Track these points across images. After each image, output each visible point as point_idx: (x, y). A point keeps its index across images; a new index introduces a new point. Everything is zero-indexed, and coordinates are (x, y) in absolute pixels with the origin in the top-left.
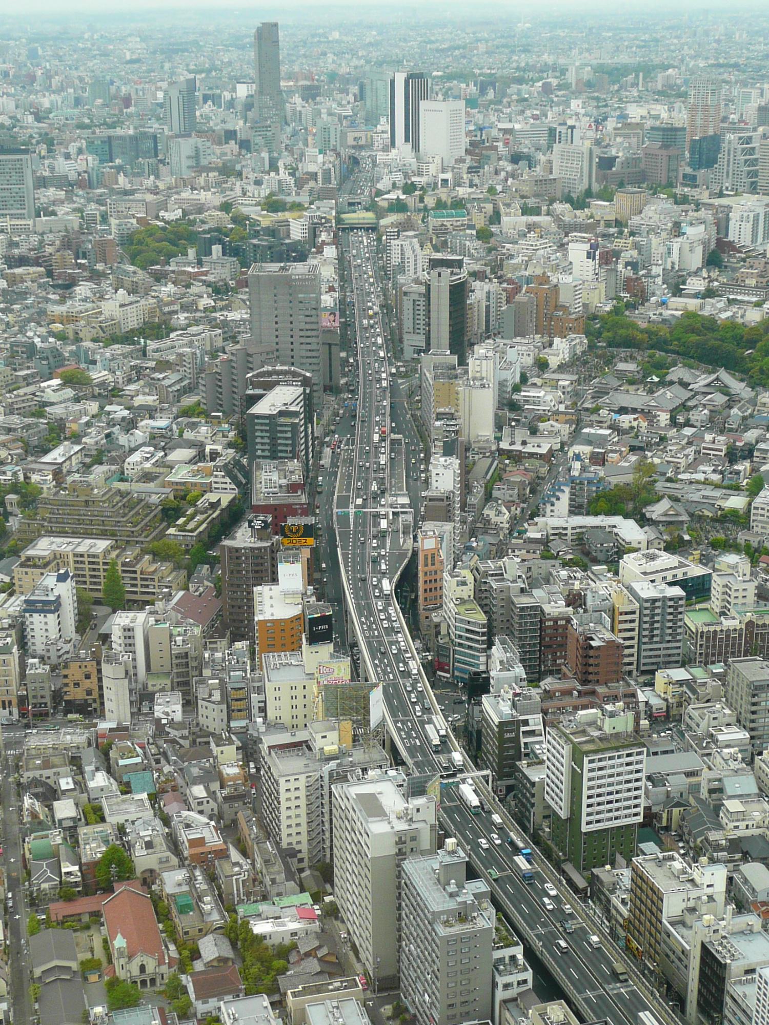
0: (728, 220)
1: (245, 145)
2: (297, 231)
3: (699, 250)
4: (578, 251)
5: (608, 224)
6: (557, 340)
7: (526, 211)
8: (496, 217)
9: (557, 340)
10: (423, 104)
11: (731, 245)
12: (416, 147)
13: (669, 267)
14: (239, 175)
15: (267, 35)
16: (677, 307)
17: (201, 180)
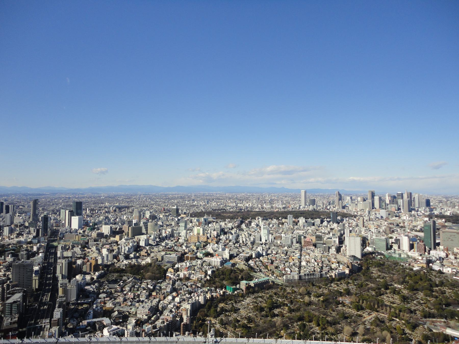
0: (140, 240)
1: (27, 227)
2: (35, 249)
3: (133, 248)
4: (105, 252)
5: (114, 243)
6: (96, 273)
7: (95, 241)
8: (87, 243)
9: (96, 273)
10: (72, 217)
11: (141, 247)
12: (71, 226)
13: (126, 252)
14: (23, 235)
15: (36, 202)
16: (126, 262)
17: (12, 237)
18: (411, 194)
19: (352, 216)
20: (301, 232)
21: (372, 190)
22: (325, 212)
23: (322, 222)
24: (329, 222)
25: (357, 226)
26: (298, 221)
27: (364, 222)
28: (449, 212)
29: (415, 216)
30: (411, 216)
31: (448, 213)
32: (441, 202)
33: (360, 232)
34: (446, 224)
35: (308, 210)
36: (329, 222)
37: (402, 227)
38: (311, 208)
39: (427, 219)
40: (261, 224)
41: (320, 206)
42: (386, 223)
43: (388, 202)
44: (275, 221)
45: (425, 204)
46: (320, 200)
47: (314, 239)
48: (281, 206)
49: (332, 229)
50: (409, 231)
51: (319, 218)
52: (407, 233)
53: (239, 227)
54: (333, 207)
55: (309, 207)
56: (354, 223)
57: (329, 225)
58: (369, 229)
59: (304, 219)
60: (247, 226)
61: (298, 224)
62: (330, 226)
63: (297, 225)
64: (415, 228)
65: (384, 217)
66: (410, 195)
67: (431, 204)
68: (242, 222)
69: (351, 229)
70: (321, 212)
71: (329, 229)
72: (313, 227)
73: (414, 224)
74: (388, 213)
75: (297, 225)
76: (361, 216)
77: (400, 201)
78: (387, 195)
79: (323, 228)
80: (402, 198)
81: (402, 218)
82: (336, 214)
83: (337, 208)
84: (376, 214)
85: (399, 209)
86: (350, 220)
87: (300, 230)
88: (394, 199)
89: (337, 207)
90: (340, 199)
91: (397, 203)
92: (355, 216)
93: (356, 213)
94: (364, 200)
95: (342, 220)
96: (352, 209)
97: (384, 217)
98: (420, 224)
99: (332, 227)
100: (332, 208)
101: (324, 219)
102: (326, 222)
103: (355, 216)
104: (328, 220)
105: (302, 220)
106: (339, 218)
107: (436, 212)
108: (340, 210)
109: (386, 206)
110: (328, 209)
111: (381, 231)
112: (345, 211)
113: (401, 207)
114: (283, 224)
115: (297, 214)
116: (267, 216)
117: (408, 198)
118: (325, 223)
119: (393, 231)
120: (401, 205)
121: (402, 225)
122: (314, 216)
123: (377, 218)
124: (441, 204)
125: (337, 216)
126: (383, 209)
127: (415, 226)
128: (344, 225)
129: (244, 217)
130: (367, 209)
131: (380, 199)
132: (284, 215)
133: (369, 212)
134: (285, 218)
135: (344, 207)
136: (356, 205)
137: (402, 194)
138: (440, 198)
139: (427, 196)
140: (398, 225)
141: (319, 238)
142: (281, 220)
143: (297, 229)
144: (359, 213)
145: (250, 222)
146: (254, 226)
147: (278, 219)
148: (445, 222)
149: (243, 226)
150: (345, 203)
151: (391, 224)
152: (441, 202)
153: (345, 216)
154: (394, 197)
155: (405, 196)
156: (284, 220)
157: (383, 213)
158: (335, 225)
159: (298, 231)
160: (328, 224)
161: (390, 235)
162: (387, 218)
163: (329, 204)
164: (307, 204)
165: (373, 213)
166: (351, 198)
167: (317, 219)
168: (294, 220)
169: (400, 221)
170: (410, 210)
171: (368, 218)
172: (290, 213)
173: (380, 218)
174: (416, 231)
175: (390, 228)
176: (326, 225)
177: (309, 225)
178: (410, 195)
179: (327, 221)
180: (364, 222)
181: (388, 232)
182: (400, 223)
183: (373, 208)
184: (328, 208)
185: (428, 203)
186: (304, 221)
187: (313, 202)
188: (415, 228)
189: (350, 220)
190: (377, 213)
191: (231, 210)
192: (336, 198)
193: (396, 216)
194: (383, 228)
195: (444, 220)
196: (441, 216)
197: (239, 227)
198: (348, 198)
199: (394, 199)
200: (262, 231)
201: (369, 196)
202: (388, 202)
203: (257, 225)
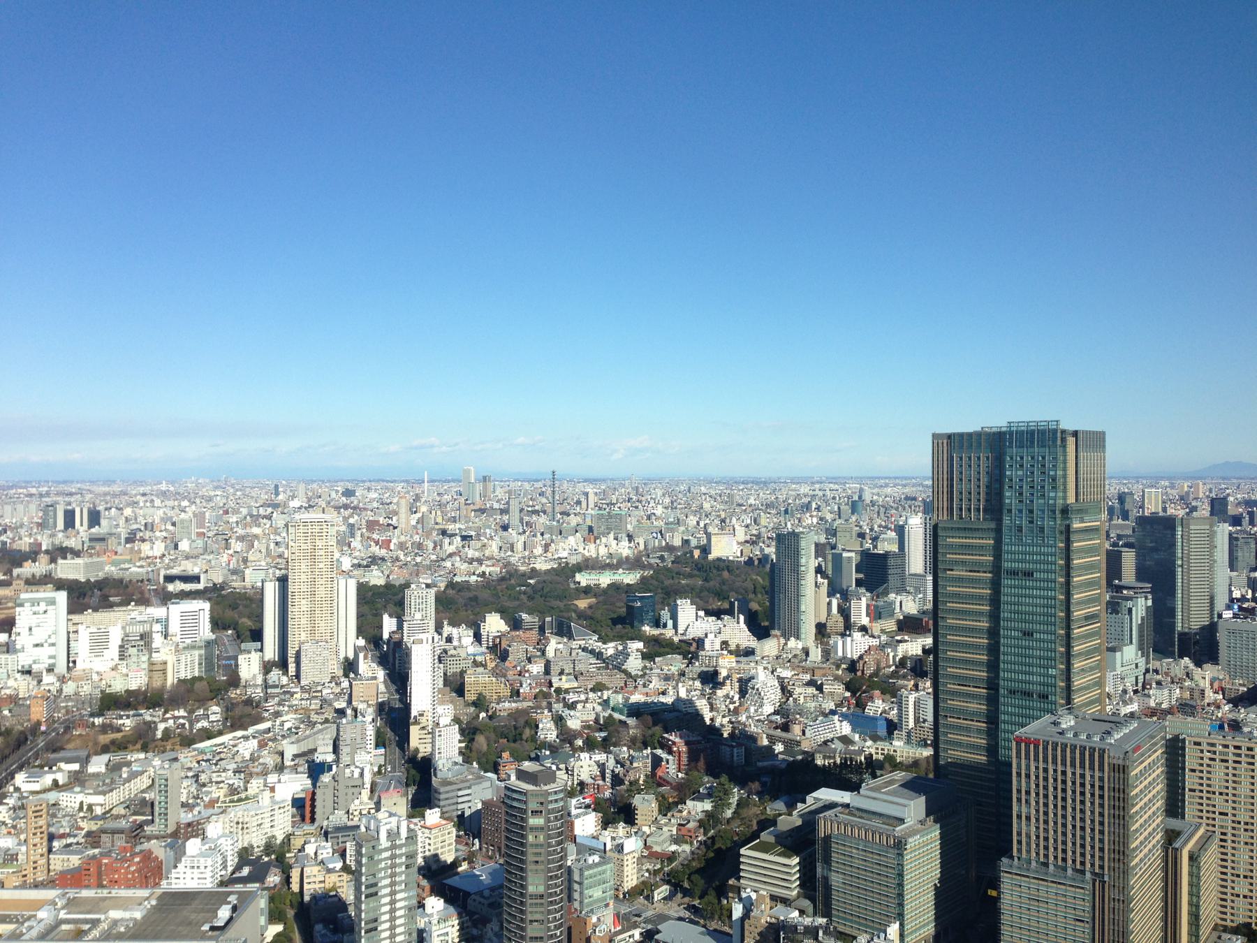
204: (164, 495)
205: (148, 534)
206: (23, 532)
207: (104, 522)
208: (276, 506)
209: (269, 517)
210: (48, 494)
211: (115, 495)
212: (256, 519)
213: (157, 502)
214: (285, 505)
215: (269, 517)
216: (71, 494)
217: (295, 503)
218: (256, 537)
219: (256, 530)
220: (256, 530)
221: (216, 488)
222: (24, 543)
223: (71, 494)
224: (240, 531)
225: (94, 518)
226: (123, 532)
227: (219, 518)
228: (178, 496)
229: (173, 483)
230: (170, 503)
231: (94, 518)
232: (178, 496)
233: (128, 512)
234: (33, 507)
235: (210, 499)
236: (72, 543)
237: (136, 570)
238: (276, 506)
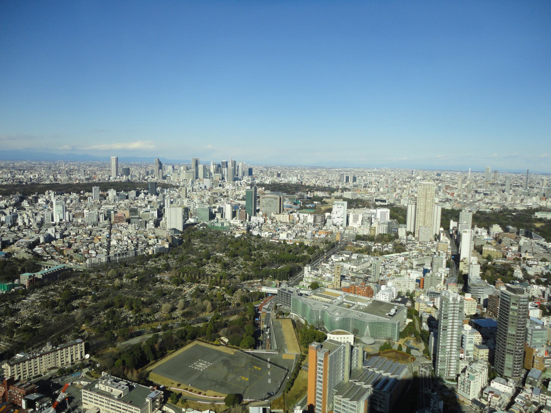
18: (235, 162)
19: (174, 187)
20: (111, 207)
21: (196, 158)
22: (142, 183)
23: (138, 194)
24: (146, 194)
25: (179, 197)
26: (108, 195)
27: (186, 193)
28: (269, 180)
29: (237, 185)
30: (234, 185)
31: (267, 182)
32: (262, 171)
33: (183, 203)
34: (265, 192)
35: (120, 182)
36: (146, 194)
37: (225, 196)
38: (124, 179)
39: (249, 188)
40: (54, 200)
41: (136, 175)
42: (209, 193)
43: (212, 171)
44: (74, 195)
45: (247, 173)
46: (137, 169)
47: (127, 214)
48: (83, 177)
49: (150, 202)
50: (232, 200)
51: (135, 190)
52: (230, 202)
53: (18, 205)
54: (152, 177)
55: (121, 178)
56: (176, 195)
57: (146, 198)
58: (192, 199)
59: (115, 191)
60: (30, 203)
61: (107, 198)
62: (148, 198)
63: (105, 199)
64: (238, 197)
65: (208, 187)
66: (234, 163)
67: (253, 173)
68: (22, 199)
69: (172, 200)
70: (138, 183)
71: (146, 202)
72: (127, 200)
73: (237, 193)
74: (211, 183)
75: (105, 199)
76: (183, 186)
77: (225, 170)
78: (212, 163)
79: (139, 202)
80: (227, 166)
81: (226, 188)
82: (156, 185)
83: (156, 179)
84: (199, 184)
85: (223, 178)
86: (171, 192)
87: (110, 205)
88: (219, 168)
89: (156, 178)
90: (161, 167)
91: (221, 172)
92: (177, 187)
93: (178, 184)
94: (187, 169)
95: (162, 191)
96: (173, 179)
97: (208, 187)
98: (242, 193)
99: (150, 200)
100: (151, 178)
101: (141, 190)
102: (143, 194)
103: (177, 187)
104: (145, 191)
105: (112, 193)
106: (158, 189)
107: (257, 181)
108: (160, 181)
109: (210, 175)
110: (145, 180)
111: (205, 201)
112: (166, 181)
113: (226, 178)
114: (86, 198)
115: (105, 187)
116: (61, 189)
117: (232, 166)
118: (142, 196)
119: (217, 201)
120: (226, 174)
121: (225, 194)
122: (129, 188)
123: (201, 188)
124: (262, 174)
125: (156, 187)
126: (207, 178)
127: (237, 195)
128: (164, 196)
129: (27, 191)
130: (191, 179)
131: (204, 168)
132: (88, 187)
133: (193, 182)
134: (89, 192)
135: (164, 178)
136: (179, 174)
137: (227, 162)
138: (261, 168)
139: (250, 166)
140: (221, 195)
141: (134, 211)
142: (83, 194)
143: (105, 204)
144: (182, 184)
145: (36, 199)
146: (42, 203)
147: (78, 192)
148: (265, 190)
149: (25, 203)
150: (165, 173)
151: (214, 193)
152: (262, 171)
153: (165, 186)
154: (219, 166)
155: (230, 164)
156: (87, 194)
157: (207, 182)
158: (154, 197)
159: (106, 206)
160: (145, 197)
161: (213, 205)
162: (211, 188)
163: (148, 174)
164: (119, 174)
165: (197, 183)
166: (173, 167)
167: (132, 191)
168: (101, 193)
169: (224, 190)
170: (235, 179)
171: (191, 188)
172: (96, 184)
173: (203, 188)
174: (239, 200)
175: (214, 198)
176: (143, 197)
177: (121, 199)
178: (234, 163)
179: (145, 193)
180: (186, 193)
181: (211, 202)
182: (224, 193)
183: (197, 178)
184: (146, 178)
185: (250, 172)
186: (115, 194)
187: (127, 172)
188: (238, 197)
189: (171, 192)
190: (201, 183)
191: (5, 183)
192: (156, 167)
193: (220, 186)
194: (207, 198)
195: (264, 188)
196: (261, 185)
197: (18, 205)
198: (170, 168)
199: (219, 168)
200: (56, 209)
201: (193, 165)
202: (212, 171)
203: (47, 202)
204: (375, 172)
205: (370, 185)
206: (334, 182)
207: (357, 181)
208: (412, 178)
209: (409, 182)
210: (341, 171)
211: (360, 172)
212: (405, 182)
213: (373, 175)
214: (415, 178)
215: (409, 182)
216: (348, 171)
217: (418, 178)
218: (405, 188)
219: (405, 186)
220: (405, 186)
221: (392, 171)
222: (334, 186)
223: (348, 171)
224: (400, 186)
225: (355, 179)
226: (363, 184)
227: (393, 181)
228: (380, 173)
229: (378, 169)
230: (377, 175)
231: (355, 179)
232: (380, 173)
233: (364, 178)
234: (337, 175)
235: (390, 175)
236: (348, 187)
237: (366, 197)
238: (412, 178)
